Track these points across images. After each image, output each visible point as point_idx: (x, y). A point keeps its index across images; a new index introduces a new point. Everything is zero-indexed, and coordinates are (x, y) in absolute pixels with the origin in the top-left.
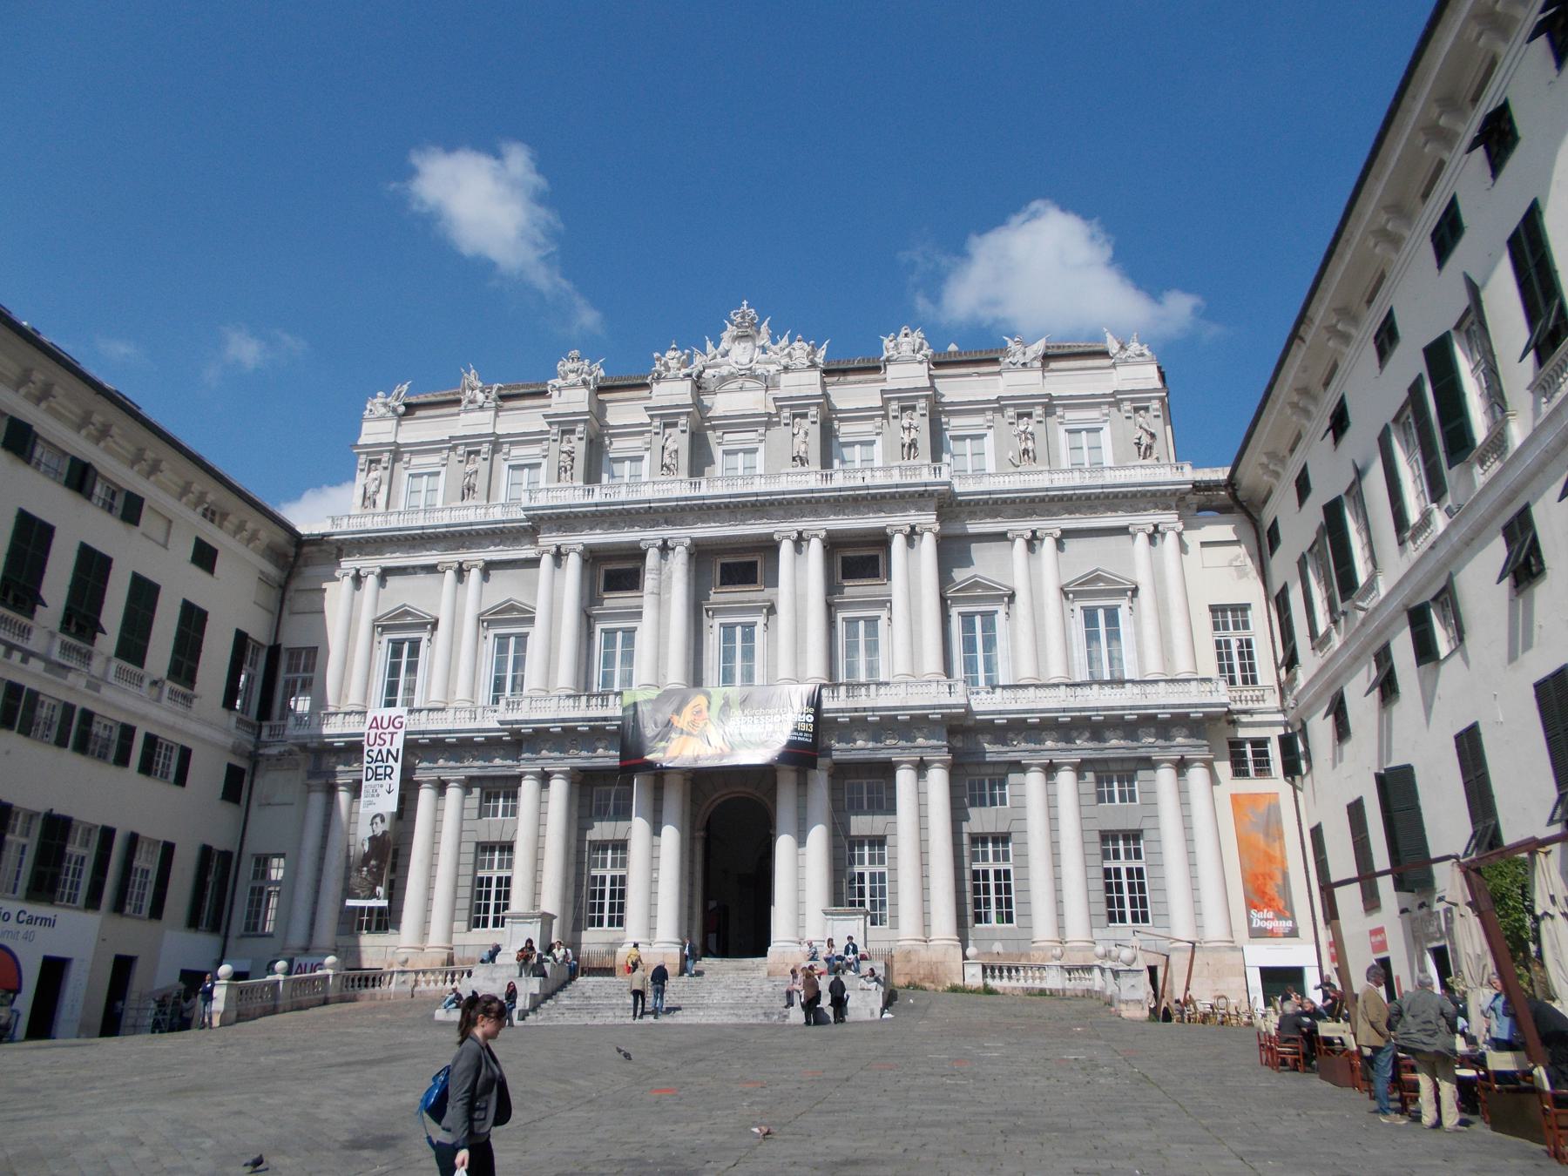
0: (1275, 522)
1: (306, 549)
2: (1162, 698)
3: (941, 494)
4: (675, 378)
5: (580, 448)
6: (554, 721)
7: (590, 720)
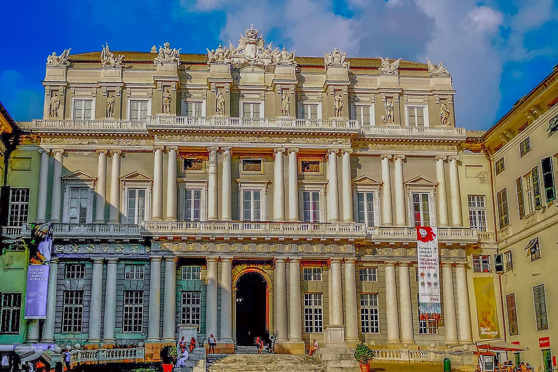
3: (354, 135)
4: (223, 63)
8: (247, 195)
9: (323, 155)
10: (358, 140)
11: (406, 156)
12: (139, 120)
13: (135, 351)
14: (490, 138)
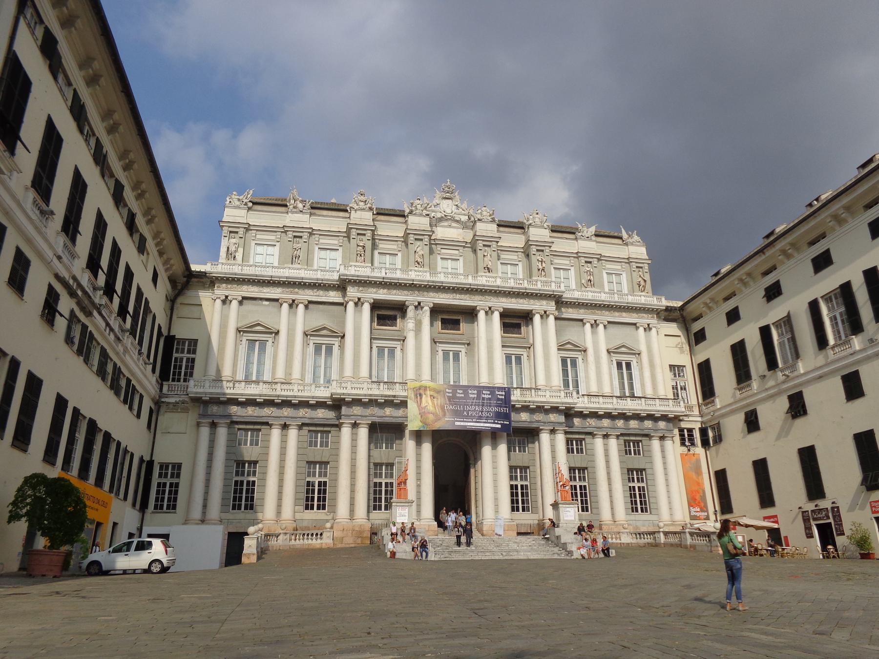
0: (702, 331)
1: (193, 279)
2: (658, 408)
4: (421, 215)
5: (369, 245)
6: (365, 395)
7: (386, 396)
8: (446, 354)
9: (527, 317)
10: (559, 301)
11: (609, 322)
13: (321, 534)
14: (691, 307)
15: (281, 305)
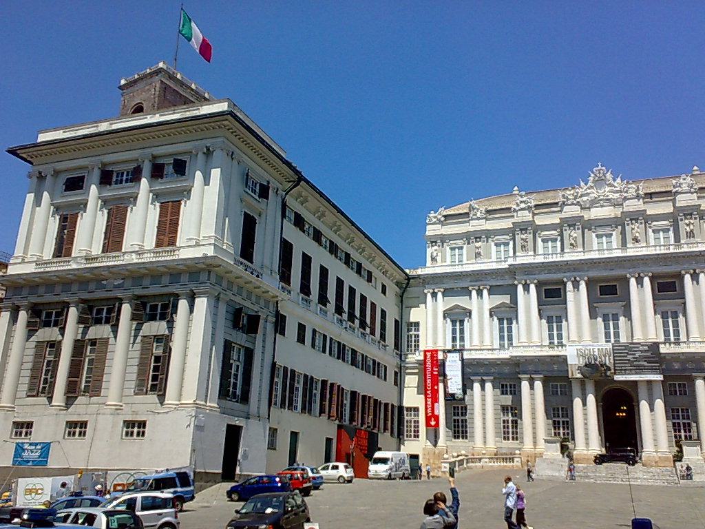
4: (573, 204)
12: (503, 259)
15: (471, 292)
